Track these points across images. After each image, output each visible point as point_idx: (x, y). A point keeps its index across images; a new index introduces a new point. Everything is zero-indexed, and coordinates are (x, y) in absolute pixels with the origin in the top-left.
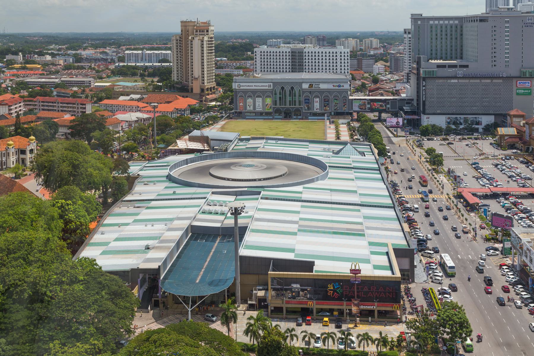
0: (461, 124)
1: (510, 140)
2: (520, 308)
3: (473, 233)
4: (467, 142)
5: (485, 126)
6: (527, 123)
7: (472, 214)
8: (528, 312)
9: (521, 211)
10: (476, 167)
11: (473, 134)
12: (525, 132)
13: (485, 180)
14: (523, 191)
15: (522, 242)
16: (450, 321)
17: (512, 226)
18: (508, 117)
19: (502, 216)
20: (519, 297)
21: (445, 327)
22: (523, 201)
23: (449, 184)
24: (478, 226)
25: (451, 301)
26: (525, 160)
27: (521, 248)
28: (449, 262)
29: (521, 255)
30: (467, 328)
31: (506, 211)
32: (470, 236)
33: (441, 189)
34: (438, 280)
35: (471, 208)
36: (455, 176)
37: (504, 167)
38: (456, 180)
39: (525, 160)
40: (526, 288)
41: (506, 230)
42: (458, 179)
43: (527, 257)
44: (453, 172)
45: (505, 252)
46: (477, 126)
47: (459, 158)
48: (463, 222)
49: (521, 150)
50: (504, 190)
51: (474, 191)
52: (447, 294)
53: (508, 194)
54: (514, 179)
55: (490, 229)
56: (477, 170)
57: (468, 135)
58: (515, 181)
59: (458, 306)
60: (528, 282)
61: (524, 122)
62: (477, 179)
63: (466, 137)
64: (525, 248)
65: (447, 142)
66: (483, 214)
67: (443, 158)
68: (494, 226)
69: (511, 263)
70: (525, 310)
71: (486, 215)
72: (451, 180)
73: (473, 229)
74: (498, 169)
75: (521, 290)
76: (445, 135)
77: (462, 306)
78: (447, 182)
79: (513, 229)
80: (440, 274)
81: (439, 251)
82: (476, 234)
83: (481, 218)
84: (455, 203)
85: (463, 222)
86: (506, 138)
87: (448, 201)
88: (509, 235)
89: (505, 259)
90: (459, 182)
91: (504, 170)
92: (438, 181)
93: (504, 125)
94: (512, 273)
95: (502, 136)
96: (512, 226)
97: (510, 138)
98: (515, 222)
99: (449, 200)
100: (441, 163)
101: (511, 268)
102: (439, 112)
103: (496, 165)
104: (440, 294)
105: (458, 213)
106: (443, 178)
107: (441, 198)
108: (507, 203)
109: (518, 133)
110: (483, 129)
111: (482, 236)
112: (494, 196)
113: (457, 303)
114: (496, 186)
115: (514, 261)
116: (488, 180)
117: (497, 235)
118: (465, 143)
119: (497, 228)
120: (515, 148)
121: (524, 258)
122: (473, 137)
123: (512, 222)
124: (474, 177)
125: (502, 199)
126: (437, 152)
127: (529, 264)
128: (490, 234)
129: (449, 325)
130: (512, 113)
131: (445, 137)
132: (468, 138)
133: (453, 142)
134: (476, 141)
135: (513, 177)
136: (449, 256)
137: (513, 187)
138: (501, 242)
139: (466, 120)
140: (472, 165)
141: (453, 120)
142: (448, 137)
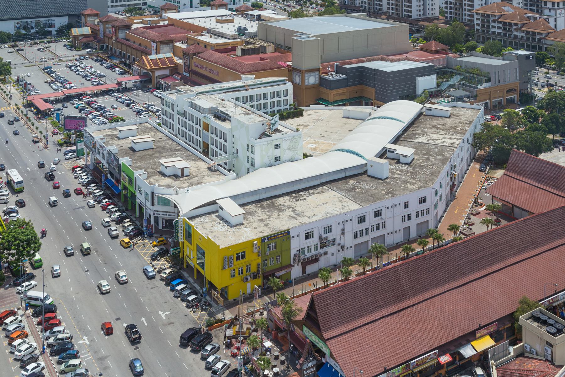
0: (32, 28)
1: (85, 40)
2: (93, 206)
3: (44, 141)
4: (39, 47)
5: (59, 28)
6: (101, 22)
7: (44, 121)
8: (101, 209)
9: (96, 110)
10: (49, 71)
11: (45, 38)
12: (99, 30)
13: (58, 84)
14: (97, 89)
15: (95, 140)
16: (16, 240)
17: (86, 126)
18: (83, 17)
19: (75, 118)
20: (91, 196)
21: (10, 250)
22: (99, 100)
23: (18, 94)
24: (49, 133)
25: (18, 219)
26: (100, 58)
27: (94, 146)
28: (16, 177)
29: (94, 153)
30: (36, 243)
31: (80, 112)
32: (41, 144)
33: (9, 100)
34: (3, 199)
35: (42, 114)
36: (25, 84)
37: (78, 68)
38: (25, 87)
39: (100, 58)
40: (99, 186)
41: (79, 131)
42: (28, 87)
43: (99, 154)
44: (23, 79)
45: (79, 154)
46: (50, 29)
47: (30, 64)
48: (33, 131)
49: (96, 49)
50: (78, 91)
51: (44, 97)
52: (14, 212)
53: (81, 95)
54: (88, 78)
55: (63, 134)
56: (49, 74)
57: (40, 39)
58: (89, 80)
59: (25, 223)
60: (101, 179)
61: (98, 20)
62: (50, 83)
63: (38, 41)
64: (98, 146)
65: (17, 48)
66: (55, 119)
67: (12, 66)
68: (67, 130)
69: (85, 163)
70: (98, 207)
71: (58, 119)
72: (21, 89)
73: (44, 137)
74: (72, 70)
75: (94, 188)
76: (13, 41)
77: (30, 221)
78: (16, 92)
79: (86, 129)
80: (6, 193)
81: (5, 168)
82: (47, 141)
83: (53, 123)
84: (25, 113)
85: (33, 131)
86: (80, 38)
87: (16, 112)
88: (82, 136)
89: (78, 161)
90: (29, 90)
91: (78, 71)
92: (5, 92)
93: (78, 25)
94: (85, 174)
95: (76, 37)
96: (86, 126)
97: (84, 38)
98: (88, 121)
99: (18, 111)
100: (9, 72)
101: (84, 168)
102: (6, 17)
103: (70, 67)
104: (5, 215)
105: (28, 123)
106: (11, 89)
107: (9, 110)
108: (81, 104)
109: (92, 32)
110: (56, 31)
111: (54, 142)
112: (68, 98)
113: (24, 219)
114: (70, 88)
115: (87, 161)
116: (61, 83)
117: (70, 138)
118: (36, 47)
119: (70, 130)
120: (90, 48)
121: (97, 156)
122: (45, 40)
123: (86, 122)
124: (46, 82)
125: (76, 101)
126: (4, 61)
127: (102, 160)
128: (63, 139)
129: (15, 245)
130: (86, 12)
131: (13, 43)
132: (40, 42)
133: (23, 48)
134: (48, 45)
135: (88, 76)
136: (17, 171)
137: (88, 87)
138: (74, 144)
139: (37, 24)
140: (44, 70)
141: (23, 25)
142: (17, 43)
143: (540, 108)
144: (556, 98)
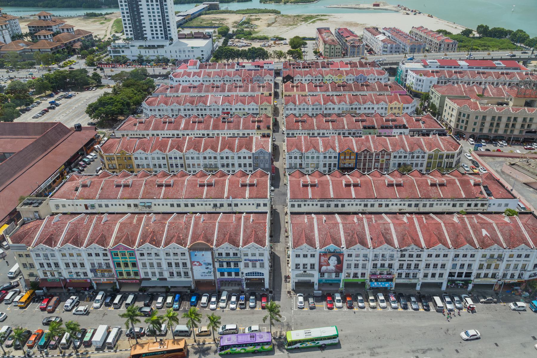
143: (7, 93)
144: (15, 85)
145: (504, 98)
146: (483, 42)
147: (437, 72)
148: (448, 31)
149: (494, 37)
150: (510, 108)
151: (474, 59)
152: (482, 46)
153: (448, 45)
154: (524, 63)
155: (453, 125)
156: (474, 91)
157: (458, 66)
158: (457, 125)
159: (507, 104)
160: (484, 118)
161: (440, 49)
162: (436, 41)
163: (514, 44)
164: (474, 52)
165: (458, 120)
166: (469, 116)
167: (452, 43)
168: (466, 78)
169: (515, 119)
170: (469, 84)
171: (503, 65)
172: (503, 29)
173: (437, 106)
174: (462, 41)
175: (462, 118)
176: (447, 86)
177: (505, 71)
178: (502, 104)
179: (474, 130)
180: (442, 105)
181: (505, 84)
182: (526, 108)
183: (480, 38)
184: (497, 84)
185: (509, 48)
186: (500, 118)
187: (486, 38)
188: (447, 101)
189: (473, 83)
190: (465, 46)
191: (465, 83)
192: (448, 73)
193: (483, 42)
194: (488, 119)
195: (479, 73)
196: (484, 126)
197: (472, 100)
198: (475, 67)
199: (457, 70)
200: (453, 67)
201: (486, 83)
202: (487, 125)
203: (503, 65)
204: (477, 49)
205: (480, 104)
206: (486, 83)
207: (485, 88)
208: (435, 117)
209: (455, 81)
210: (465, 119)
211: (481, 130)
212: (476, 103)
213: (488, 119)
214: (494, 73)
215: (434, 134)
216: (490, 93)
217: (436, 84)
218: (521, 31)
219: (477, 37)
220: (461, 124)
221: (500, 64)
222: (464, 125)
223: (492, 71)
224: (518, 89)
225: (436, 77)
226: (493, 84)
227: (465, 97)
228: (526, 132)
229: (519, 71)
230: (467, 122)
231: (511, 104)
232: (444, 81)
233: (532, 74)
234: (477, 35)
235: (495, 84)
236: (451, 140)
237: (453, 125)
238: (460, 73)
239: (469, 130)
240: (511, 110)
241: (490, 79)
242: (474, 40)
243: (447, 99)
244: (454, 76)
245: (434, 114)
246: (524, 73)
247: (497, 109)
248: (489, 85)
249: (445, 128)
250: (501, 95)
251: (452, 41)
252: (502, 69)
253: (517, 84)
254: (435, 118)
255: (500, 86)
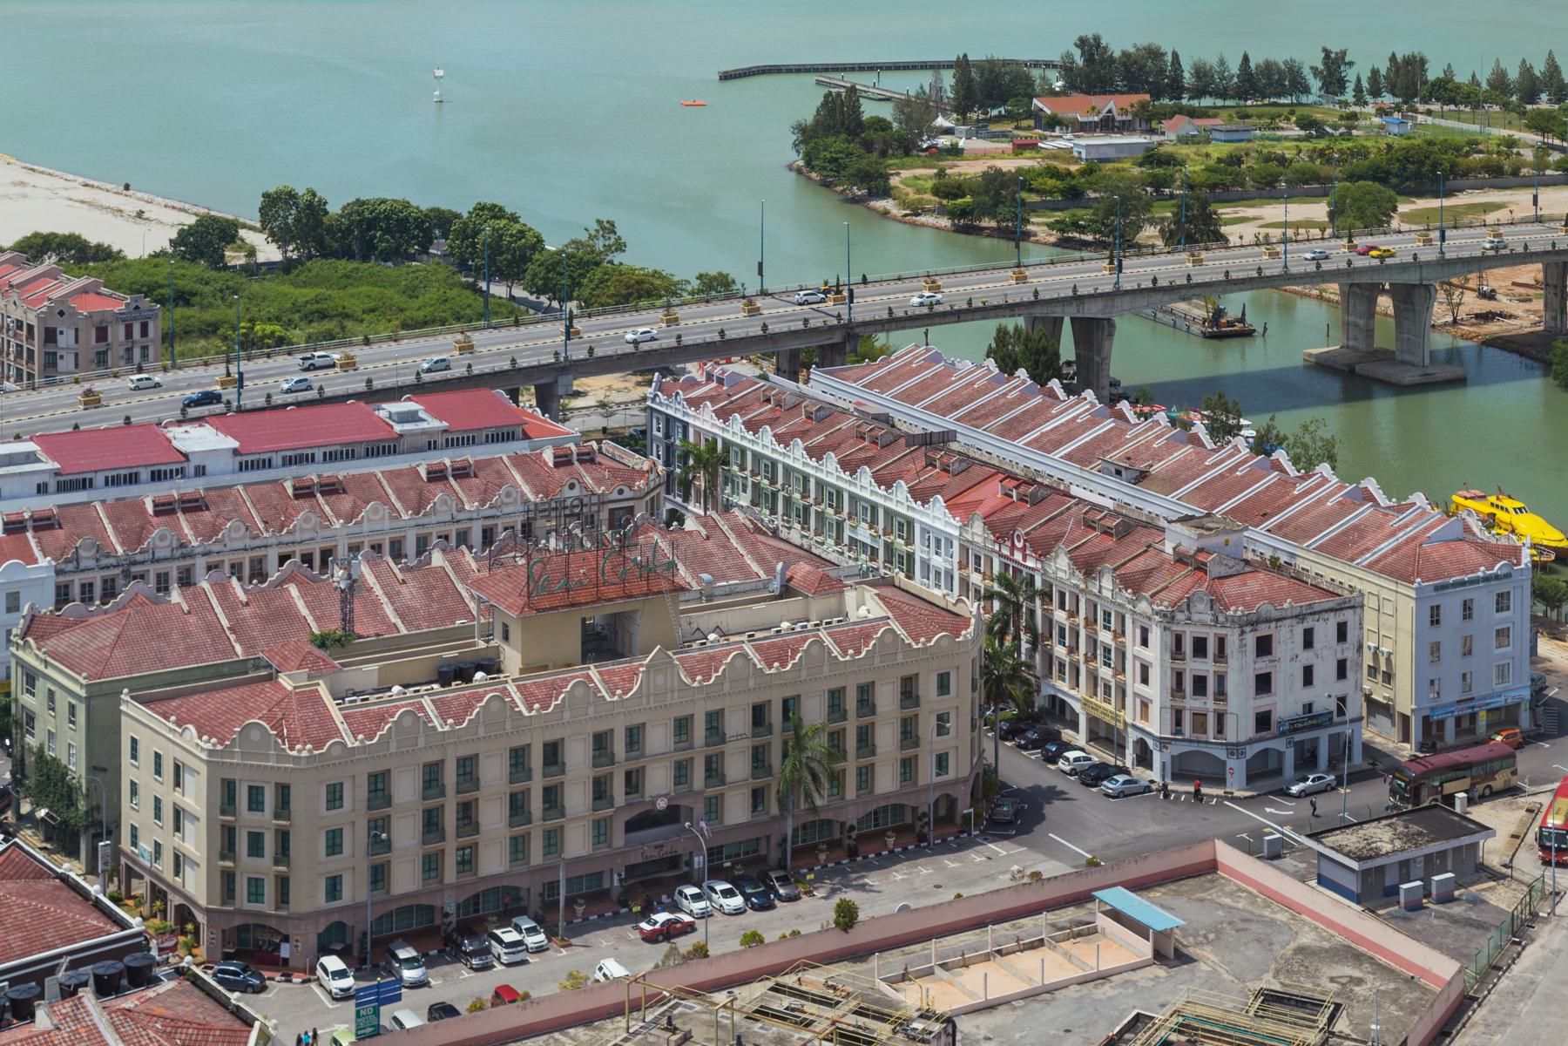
145: (466, 632)
146: (309, 293)
147: (44, 523)
148: (93, 238)
149: (365, 259)
150: (511, 688)
151: (270, 407)
152: (309, 318)
153: (102, 334)
154: (547, 400)
155: (196, 885)
156: (289, 613)
157: (180, 465)
158: (228, 878)
159: (492, 666)
160: (379, 786)
161: (51, 362)
162: (17, 314)
163: (474, 288)
164: (261, 363)
165: (226, 841)
166: (284, 792)
167: (119, 317)
168: (233, 534)
169: (553, 753)
170: (259, 573)
171: (433, 423)
172: (407, 205)
173: (77, 769)
174: (183, 298)
175: (247, 820)
176: (120, 609)
177: (446, 459)
178: (462, 673)
179: (333, 887)
180: (104, 763)
181: (463, 538)
182: (593, 672)
183: (287, 267)
184: (423, 545)
185: (458, 319)
186: (468, 768)
187: (318, 266)
188: (137, 720)
189: (283, 559)
190: (210, 330)
191: (236, 569)
192: (115, 521)
193: (309, 293)
194: (406, 788)
195: (304, 492)
196: (387, 846)
197: (285, 682)
198: (277, 459)
199: (173, 489)
200: (145, 474)
201: (354, 549)
202: (406, 833)
203: (433, 423)
204: (281, 341)
205: (338, 697)
206: (354, 549)
207: (354, 585)
208: (73, 853)
209: (173, 569)
210: (265, 820)
211: (379, 875)
212: (315, 697)
213: (406, 788)
214: (392, 476)
215: (68, 992)
216: (389, 610)
217: (47, 607)
218: (496, 212)
219: (271, 266)
220: (247, 866)
221: (411, 417)
222: (265, 866)
223: (377, 467)
224: (529, 557)
225: (44, 562)
226: (397, 553)
227: (241, 667)
228: (631, 826)
229: (521, 447)
230: (284, 838)
231: (512, 659)
232: (97, 578)
233: (588, 459)
234: (269, 252)
235: (410, 547)
236: (194, 1007)
237: (196, 885)
238: (193, 505)
239: (309, 897)
240: (517, 697)
241: (375, 520)
242: (256, 287)
243: (130, 707)
244: (158, 536)
245: (63, 838)
246: (548, 456)
247: (443, 709)
248: (372, 564)
249: (136, 924)
250: (453, 615)
251: (118, 304)
252: (432, 446)
253: (527, 529)
254: (72, 869)
255: (438, 559)
